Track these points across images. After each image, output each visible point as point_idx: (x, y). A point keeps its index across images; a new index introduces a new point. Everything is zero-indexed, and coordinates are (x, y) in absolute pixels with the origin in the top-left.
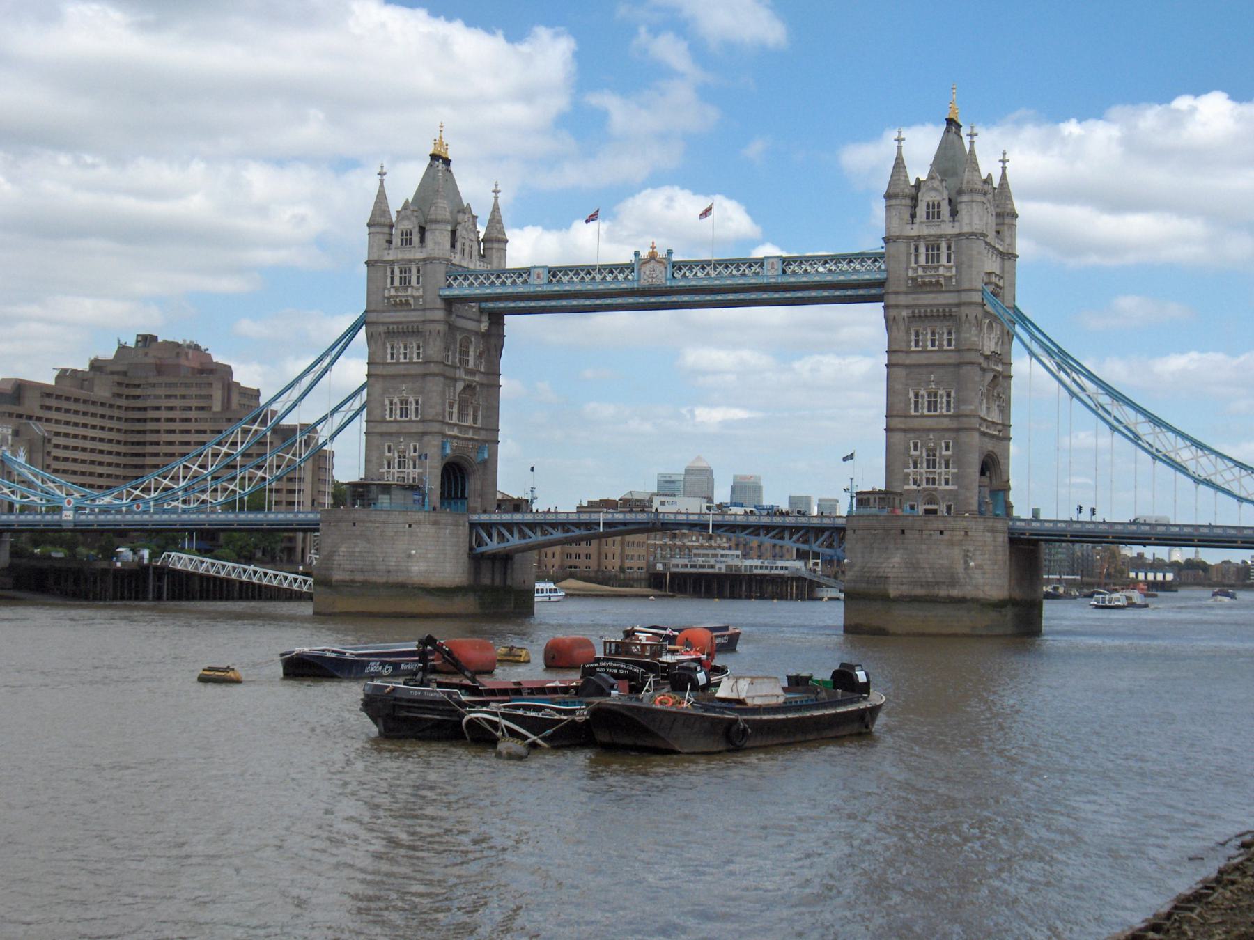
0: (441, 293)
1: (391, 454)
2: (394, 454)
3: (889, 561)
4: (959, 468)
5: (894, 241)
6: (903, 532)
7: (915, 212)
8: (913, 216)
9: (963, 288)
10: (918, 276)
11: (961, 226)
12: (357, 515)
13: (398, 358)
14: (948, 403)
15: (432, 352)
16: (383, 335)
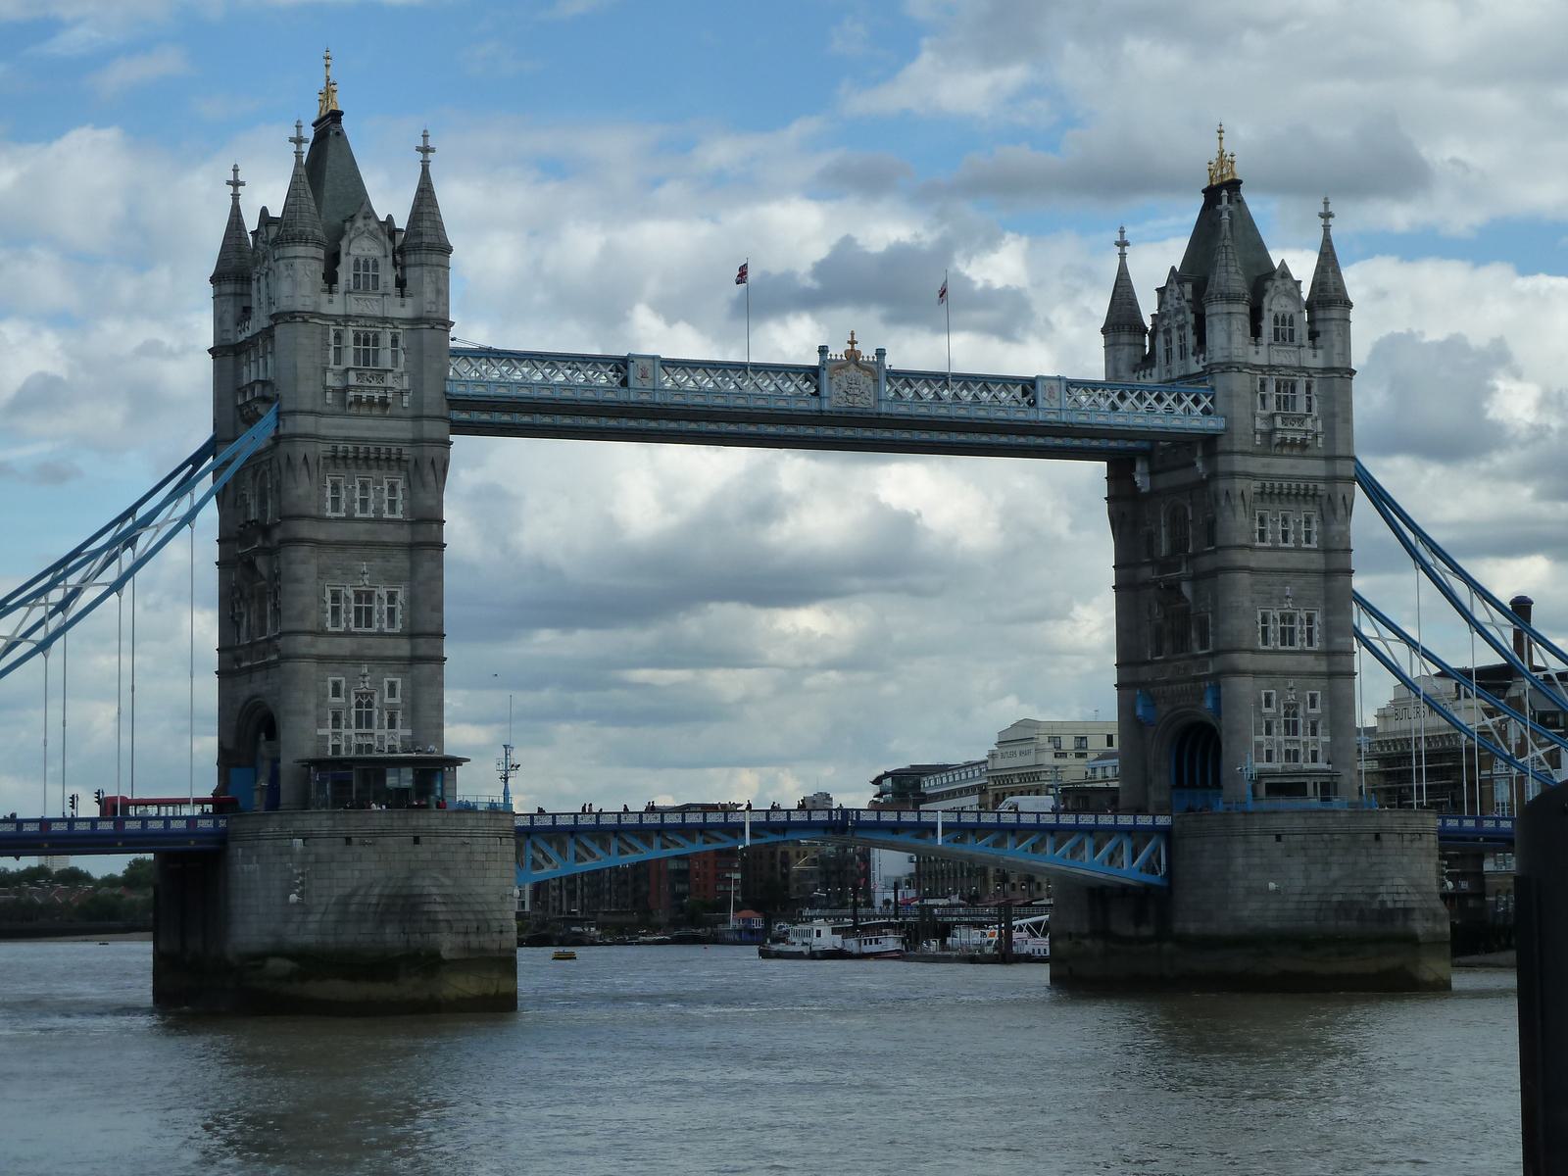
0: (448, 389)
2: (348, 697)
3: (1388, 882)
4: (1333, 735)
5: (1241, 372)
6: (1377, 837)
7: (1261, 327)
8: (1256, 332)
9: (1341, 451)
10: (1280, 429)
11: (1328, 356)
12: (422, 822)
13: (350, 508)
14: (1310, 631)
15: (431, 502)
16: (321, 459)
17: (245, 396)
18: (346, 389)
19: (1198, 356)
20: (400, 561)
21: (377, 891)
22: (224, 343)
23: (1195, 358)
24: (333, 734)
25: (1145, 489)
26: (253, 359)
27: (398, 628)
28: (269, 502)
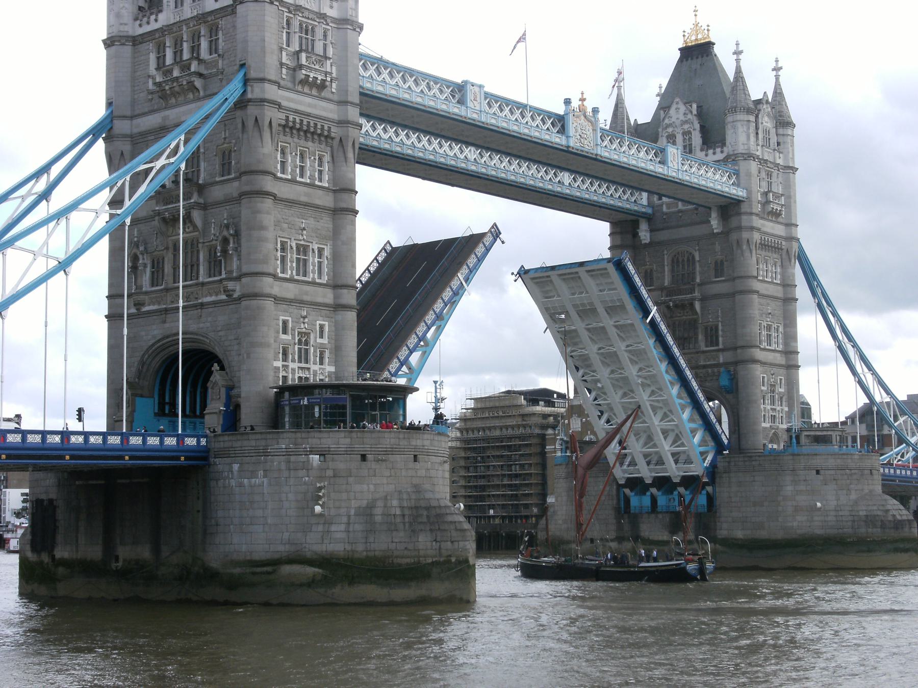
1: (289, 337)
2: (294, 338)
5: (754, 160)
9: (793, 222)
11: (786, 158)
12: (419, 443)
17: (170, 71)
18: (301, 67)
19: (707, 150)
20: (326, 223)
21: (395, 503)
22: (125, 34)
23: (704, 153)
24: (283, 366)
25: (647, 241)
26: (168, 44)
27: (325, 279)
28: (202, 165)
